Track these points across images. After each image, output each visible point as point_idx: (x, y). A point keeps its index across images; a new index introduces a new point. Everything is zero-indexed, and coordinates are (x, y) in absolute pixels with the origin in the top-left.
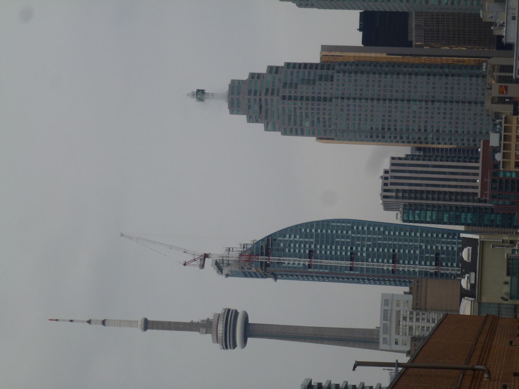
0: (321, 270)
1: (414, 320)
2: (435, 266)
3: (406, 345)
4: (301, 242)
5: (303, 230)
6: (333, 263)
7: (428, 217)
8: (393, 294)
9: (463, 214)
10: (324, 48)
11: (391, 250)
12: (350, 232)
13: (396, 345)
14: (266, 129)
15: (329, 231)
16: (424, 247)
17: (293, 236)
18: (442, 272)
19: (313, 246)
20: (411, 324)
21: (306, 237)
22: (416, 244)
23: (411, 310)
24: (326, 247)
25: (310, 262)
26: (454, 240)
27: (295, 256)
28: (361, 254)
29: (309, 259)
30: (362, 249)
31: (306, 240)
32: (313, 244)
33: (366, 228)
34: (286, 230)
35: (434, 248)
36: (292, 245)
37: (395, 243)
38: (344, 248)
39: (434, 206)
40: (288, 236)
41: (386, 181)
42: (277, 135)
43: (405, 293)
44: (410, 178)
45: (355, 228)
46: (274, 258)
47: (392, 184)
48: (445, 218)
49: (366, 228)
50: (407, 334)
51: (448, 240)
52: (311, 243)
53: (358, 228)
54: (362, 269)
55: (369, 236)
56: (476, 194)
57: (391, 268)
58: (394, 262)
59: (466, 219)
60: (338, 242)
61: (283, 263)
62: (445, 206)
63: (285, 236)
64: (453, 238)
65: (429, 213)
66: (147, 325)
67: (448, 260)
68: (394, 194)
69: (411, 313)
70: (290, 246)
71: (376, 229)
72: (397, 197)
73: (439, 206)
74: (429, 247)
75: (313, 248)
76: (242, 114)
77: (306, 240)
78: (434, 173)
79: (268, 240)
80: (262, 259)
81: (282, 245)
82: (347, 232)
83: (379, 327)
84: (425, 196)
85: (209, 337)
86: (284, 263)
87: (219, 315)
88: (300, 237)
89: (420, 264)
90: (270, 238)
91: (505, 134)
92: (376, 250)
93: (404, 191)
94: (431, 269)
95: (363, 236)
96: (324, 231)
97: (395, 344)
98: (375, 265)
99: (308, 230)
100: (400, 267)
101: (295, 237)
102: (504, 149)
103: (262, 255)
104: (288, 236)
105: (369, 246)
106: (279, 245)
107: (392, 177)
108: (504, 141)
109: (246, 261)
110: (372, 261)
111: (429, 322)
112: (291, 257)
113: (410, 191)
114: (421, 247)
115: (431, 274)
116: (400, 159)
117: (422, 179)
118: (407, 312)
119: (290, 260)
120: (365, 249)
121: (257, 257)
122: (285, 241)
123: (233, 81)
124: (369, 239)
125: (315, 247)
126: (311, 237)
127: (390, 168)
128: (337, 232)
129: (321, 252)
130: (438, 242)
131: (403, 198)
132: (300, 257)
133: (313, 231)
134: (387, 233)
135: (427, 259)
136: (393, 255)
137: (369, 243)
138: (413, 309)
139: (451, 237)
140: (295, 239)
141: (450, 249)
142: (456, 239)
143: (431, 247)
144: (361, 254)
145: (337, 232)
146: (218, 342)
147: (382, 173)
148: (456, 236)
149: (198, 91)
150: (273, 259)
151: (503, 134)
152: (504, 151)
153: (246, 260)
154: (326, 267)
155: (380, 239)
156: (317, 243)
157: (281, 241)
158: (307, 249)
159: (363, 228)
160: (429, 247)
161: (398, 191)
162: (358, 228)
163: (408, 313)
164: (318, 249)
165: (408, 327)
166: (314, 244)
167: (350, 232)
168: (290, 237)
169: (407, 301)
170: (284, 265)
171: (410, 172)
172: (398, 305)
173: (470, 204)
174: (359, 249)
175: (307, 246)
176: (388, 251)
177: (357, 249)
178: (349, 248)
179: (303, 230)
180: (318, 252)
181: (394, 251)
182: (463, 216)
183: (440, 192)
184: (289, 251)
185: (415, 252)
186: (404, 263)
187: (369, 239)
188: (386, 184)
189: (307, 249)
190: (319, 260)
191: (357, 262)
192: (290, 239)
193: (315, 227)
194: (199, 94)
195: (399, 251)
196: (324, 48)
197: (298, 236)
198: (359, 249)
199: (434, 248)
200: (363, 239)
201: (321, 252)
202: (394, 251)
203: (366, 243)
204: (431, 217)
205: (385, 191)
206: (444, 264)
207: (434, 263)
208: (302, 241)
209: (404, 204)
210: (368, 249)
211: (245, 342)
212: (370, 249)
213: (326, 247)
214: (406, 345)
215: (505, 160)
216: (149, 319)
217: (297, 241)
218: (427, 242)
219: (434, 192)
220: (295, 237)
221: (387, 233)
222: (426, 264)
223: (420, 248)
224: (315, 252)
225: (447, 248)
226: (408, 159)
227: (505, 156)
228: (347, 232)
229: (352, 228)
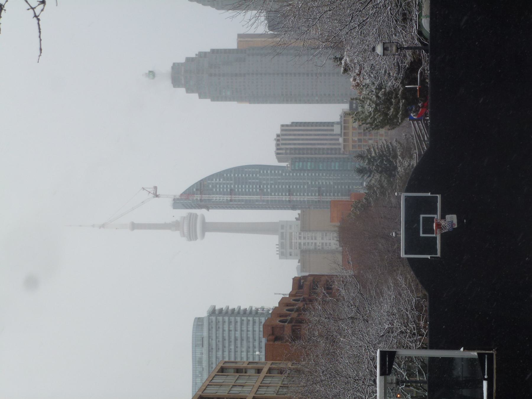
0: (239, 203)
1: (302, 238)
2: (318, 196)
3: (297, 256)
4: (224, 184)
5: (225, 175)
6: (247, 197)
7: (308, 167)
8: (287, 221)
9: (332, 163)
10: (240, 36)
11: (287, 187)
12: (258, 175)
13: (291, 256)
14: (200, 97)
15: (244, 175)
16: (310, 183)
17: (218, 180)
18: (323, 200)
19: (232, 186)
20: (300, 241)
23: (300, 232)
24: (242, 187)
25: (231, 197)
26: (331, 177)
27: (221, 194)
28: (267, 190)
29: (230, 195)
30: (267, 187)
31: (228, 182)
32: (232, 184)
33: (269, 172)
34: (213, 175)
35: (317, 183)
36: (218, 186)
37: (290, 181)
38: (254, 186)
39: (312, 158)
40: (214, 180)
41: (278, 142)
42: (207, 102)
43: (296, 218)
45: (262, 172)
46: (205, 196)
47: (283, 144)
48: (320, 166)
49: (269, 172)
50: (298, 248)
51: (327, 177)
52: (231, 184)
53: (263, 172)
54: (268, 201)
55: (271, 177)
56: (340, 149)
57: (287, 199)
58: (289, 195)
59: (335, 167)
60: (250, 183)
61: (212, 199)
62: (320, 158)
63: (212, 180)
64: (330, 176)
65: (309, 164)
66: (134, 226)
68: (284, 151)
69: (300, 234)
70: (216, 187)
71: (277, 172)
72: (286, 154)
73: (316, 158)
74: (313, 183)
75: (232, 188)
76: (182, 87)
77: (228, 182)
78: (311, 135)
79: (201, 184)
80: (198, 197)
81: (210, 186)
82: (256, 175)
83: (278, 244)
84: (305, 152)
85: (177, 233)
86: (213, 199)
87: (184, 217)
88: (223, 180)
89: (308, 195)
90: (202, 181)
91: (345, 125)
92: (277, 186)
93: (291, 149)
94: (315, 198)
95: (268, 177)
96: (240, 175)
97: (289, 255)
98: (277, 198)
99: (229, 175)
100: (294, 198)
101: (220, 180)
102: (344, 136)
103: (197, 194)
104: (214, 180)
105: (271, 184)
107: (283, 140)
108: (344, 130)
109: (186, 199)
110: (275, 195)
111: (313, 239)
112: (218, 194)
113: (295, 149)
114: (308, 183)
115: (316, 202)
116: (287, 126)
117: (303, 140)
118: (297, 233)
119: (216, 197)
120: (269, 186)
121: (193, 196)
122: (212, 183)
123: (174, 64)
124: (271, 179)
125: (234, 186)
126: (231, 180)
127: (280, 132)
128: (249, 175)
129: (238, 190)
131: (291, 154)
132: (224, 195)
133: (232, 175)
134: (284, 174)
136: (289, 190)
137: (272, 182)
138: (301, 230)
139: (328, 175)
141: (328, 183)
143: (315, 183)
144: (267, 190)
145: (249, 175)
146: (184, 236)
147: (275, 137)
149: (150, 72)
150: (205, 197)
151: (343, 125)
152: (344, 137)
153: (185, 198)
154: (242, 200)
155: (279, 179)
157: (210, 183)
158: (229, 188)
159: (267, 172)
160: (313, 183)
161: (287, 149)
162: (263, 172)
163: (298, 233)
164: (236, 188)
165: (298, 243)
166: (233, 184)
167: (258, 175)
168: (216, 180)
169: (297, 226)
170: (213, 200)
171: (295, 135)
172: (291, 228)
173: (337, 156)
174: (265, 186)
175: (229, 186)
176: (286, 187)
177: (263, 187)
178: (258, 186)
179: (225, 175)
180: (236, 190)
181: (289, 187)
182: (333, 164)
183: (316, 149)
184: (216, 190)
185: (304, 187)
186: (297, 195)
187: (271, 179)
188: (278, 145)
189: (229, 188)
190: (237, 196)
191: (264, 196)
192: (216, 182)
193: (233, 172)
194: (151, 74)
195: (293, 187)
196: (240, 36)
197: (221, 180)
198: (265, 186)
199: (317, 183)
201: (238, 190)
202: (289, 187)
203: (269, 182)
204: (311, 166)
205: (278, 149)
206: (324, 194)
207: (317, 194)
208: (225, 183)
209: (291, 158)
210: (271, 186)
211: (203, 236)
212: (273, 186)
213: (242, 187)
214: (297, 256)
215: (344, 143)
216: (135, 222)
217: (221, 183)
219: (311, 149)
220: (220, 180)
221: (284, 174)
222: (312, 195)
223: (307, 183)
225: (326, 183)
226: (293, 126)
227: (345, 141)
228: (256, 175)
229: (260, 172)
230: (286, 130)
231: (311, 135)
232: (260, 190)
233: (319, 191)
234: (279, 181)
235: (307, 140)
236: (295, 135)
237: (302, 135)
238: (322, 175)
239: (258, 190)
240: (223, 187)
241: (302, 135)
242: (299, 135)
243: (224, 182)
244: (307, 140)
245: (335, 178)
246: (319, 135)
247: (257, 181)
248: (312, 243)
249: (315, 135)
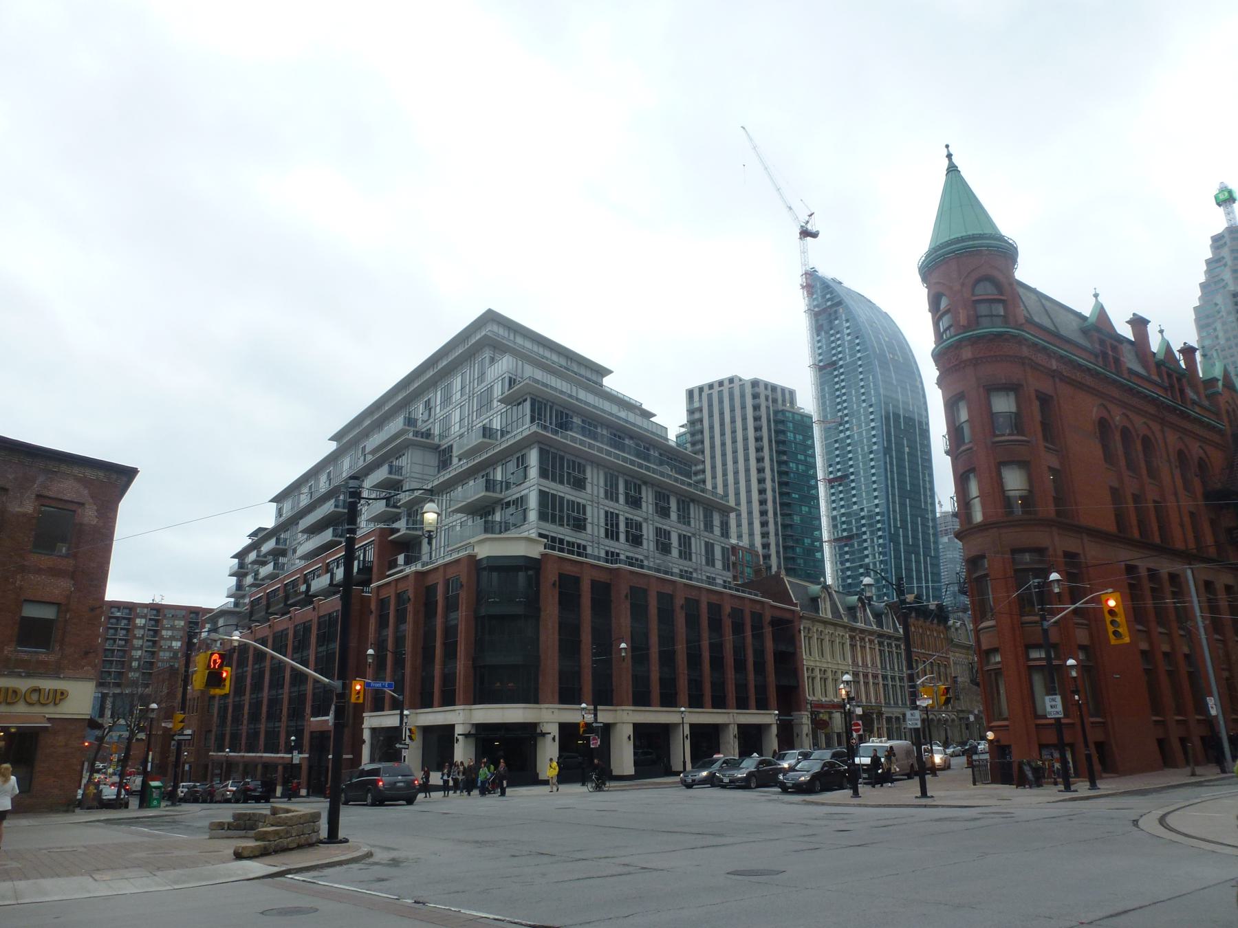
4: (844, 346)
5: (857, 341)
16: (862, 514)
17: (848, 331)
19: (841, 363)
21: (851, 349)
22: (865, 502)
26: (877, 555)
35: (864, 529)
36: (838, 336)
40: (848, 324)
44: (722, 424)
45: (871, 410)
47: (710, 396)
63: (847, 321)
67: (852, 553)
70: (838, 333)
74: (863, 522)
81: (837, 322)
82: (864, 401)
93: (701, 420)
101: (848, 334)
104: (848, 324)
106: (836, 319)
114: (862, 510)
117: (723, 444)
125: (841, 367)
126: (851, 356)
130: (872, 533)
133: (859, 355)
134: (872, 456)
135: (849, 523)
140: (846, 336)
142: (879, 558)
148: (883, 557)
155: (863, 449)
156: (847, 365)
160: (863, 522)
161: (700, 410)
162: (872, 413)
167: (864, 405)
168: (848, 328)
171: (733, 421)
175: (840, 356)
177: (847, 422)
179: (857, 341)
184: (832, 335)
199: (864, 529)
200: (859, 426)
205: (701, 389)
210: (848, 437)
212: (848, 441)
218: (870, 517)
220: (848, 334)
224: (835, 370)
228: (864, 401)
229: (871, 406)
230: (743, 396)
231: (735, 462)
232: (841, 416)
233: (850, 538)
234: (859, 449)
235: (724, 455)
236: (733, 421)
237: (734, 441)
238: (880, 537)
239: (840, 414)
240: (839, 346)
241: (734, 441)
242: (734, 432)
243: (846, 343)
244: (724, 455)
245: (878, 563)
246: (737, 482)
247: (855, 406)
248: (579, 525)
249: (736, 473)
